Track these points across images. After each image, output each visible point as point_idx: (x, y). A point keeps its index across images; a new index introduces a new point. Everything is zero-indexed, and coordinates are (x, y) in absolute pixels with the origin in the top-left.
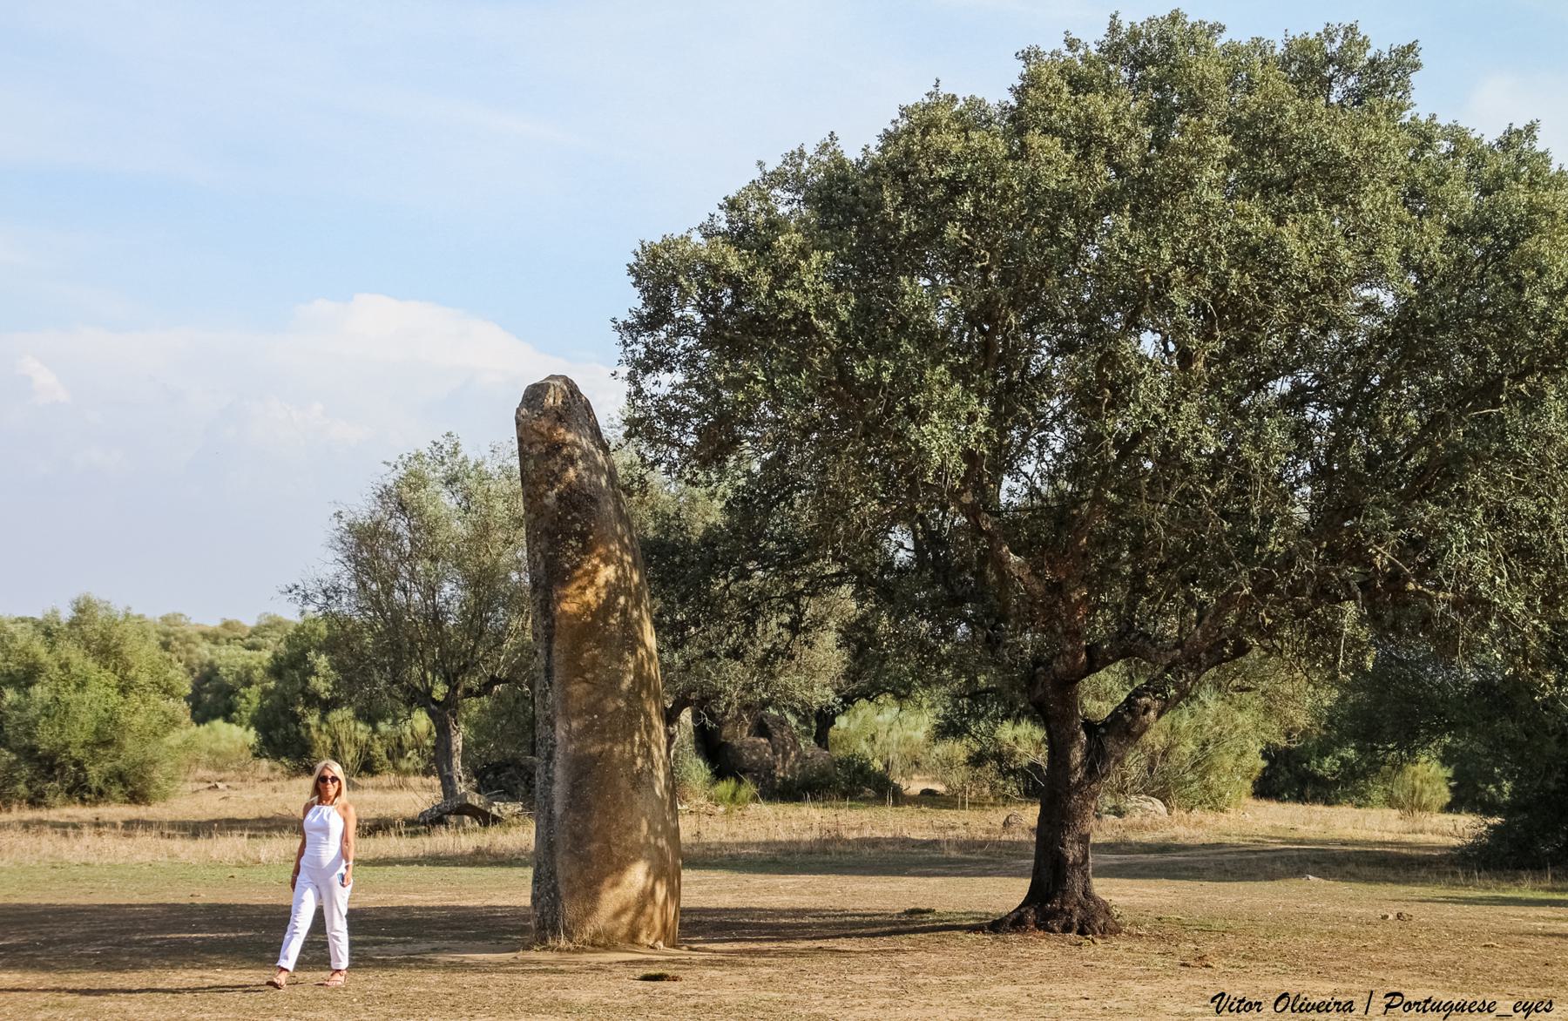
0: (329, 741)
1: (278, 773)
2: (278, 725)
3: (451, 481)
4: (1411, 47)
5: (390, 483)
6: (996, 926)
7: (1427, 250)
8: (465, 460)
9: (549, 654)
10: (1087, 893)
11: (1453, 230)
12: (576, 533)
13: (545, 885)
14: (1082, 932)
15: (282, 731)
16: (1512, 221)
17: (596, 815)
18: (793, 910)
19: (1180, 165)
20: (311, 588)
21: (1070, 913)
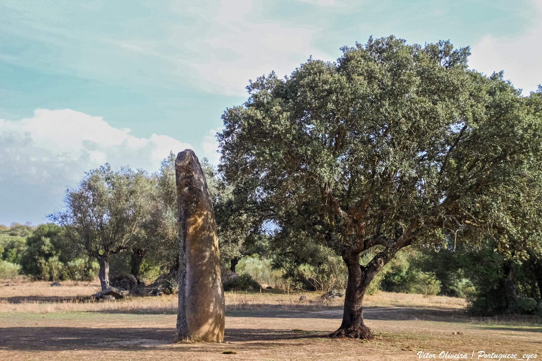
0: (48, 268)
1: (26, 280)
2: (28, 263)
3: (107, 179)
4: (467, 48)
5: (86, 180)
6: (332, 336)
7: (480, 114)
8: (112, 172)
9: (185, 241)
10: (362, 325)
11: (487, 107)
12: (194, 201)
13: (181, 319)
14: (361, 338)
15: (30, 265)
16: (506, 105)
17: (200, 297)
18: (264, 330)
19: (404, 86)
20: (57, 215)
21: (357, 331)
